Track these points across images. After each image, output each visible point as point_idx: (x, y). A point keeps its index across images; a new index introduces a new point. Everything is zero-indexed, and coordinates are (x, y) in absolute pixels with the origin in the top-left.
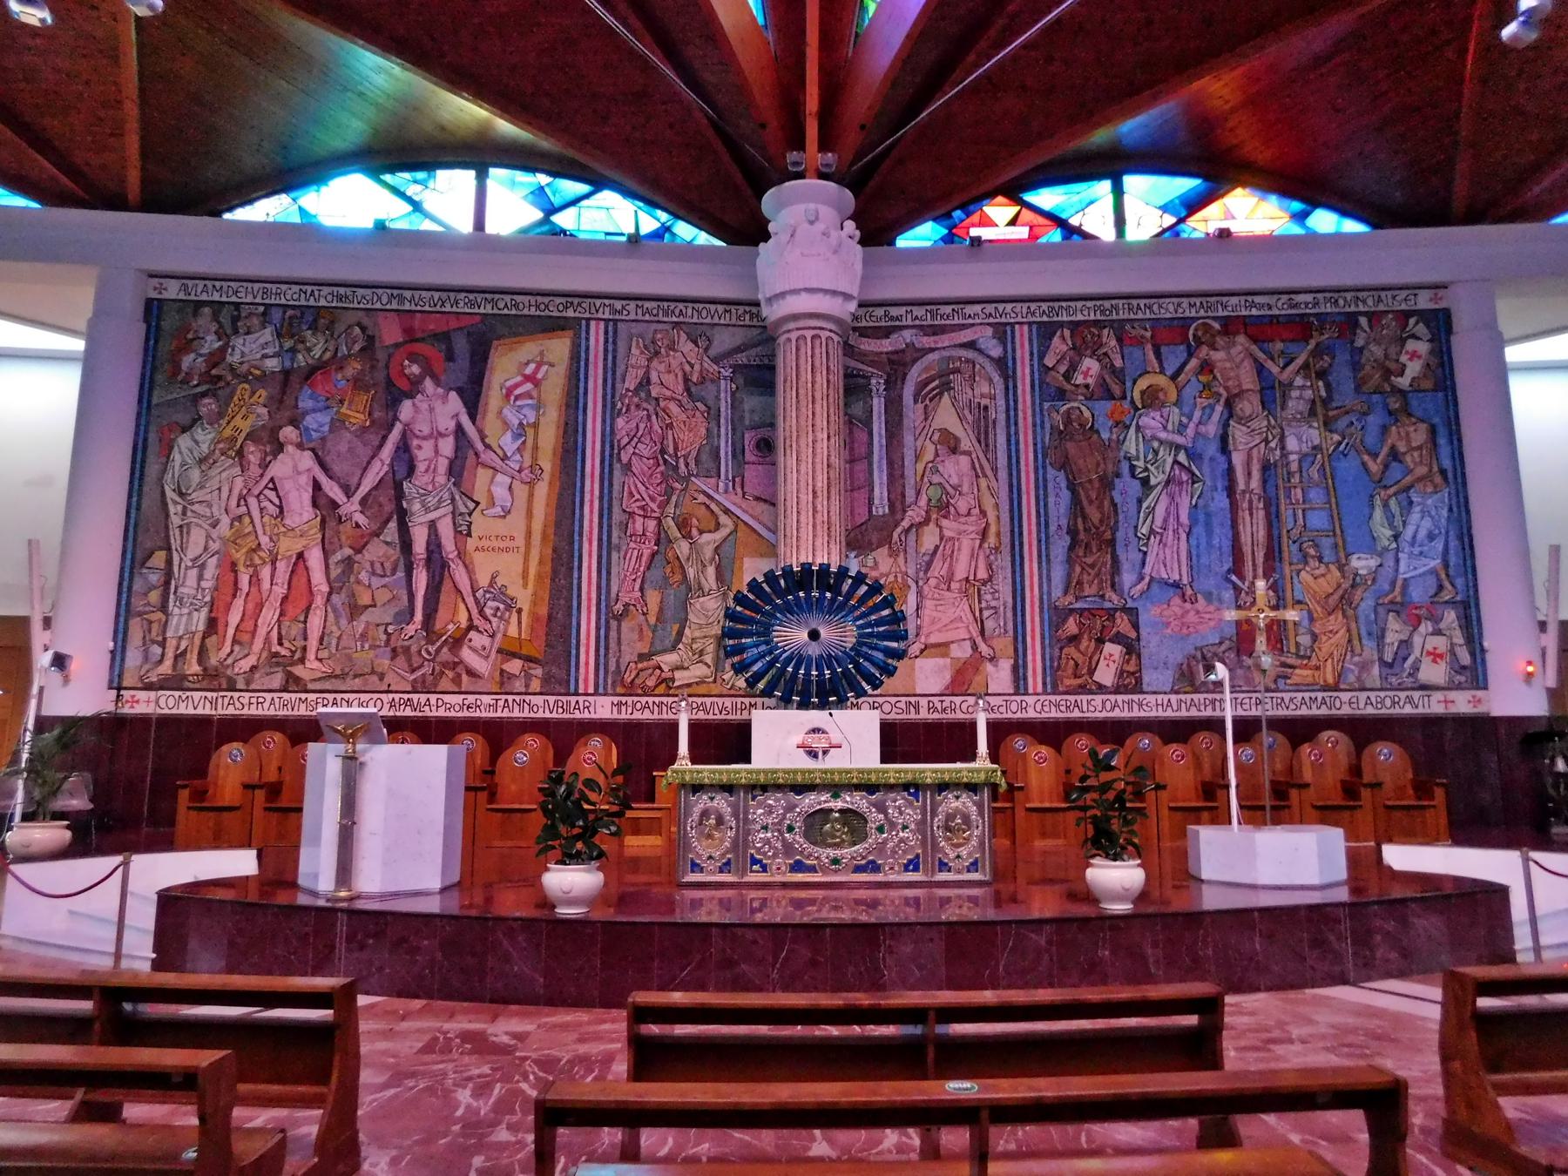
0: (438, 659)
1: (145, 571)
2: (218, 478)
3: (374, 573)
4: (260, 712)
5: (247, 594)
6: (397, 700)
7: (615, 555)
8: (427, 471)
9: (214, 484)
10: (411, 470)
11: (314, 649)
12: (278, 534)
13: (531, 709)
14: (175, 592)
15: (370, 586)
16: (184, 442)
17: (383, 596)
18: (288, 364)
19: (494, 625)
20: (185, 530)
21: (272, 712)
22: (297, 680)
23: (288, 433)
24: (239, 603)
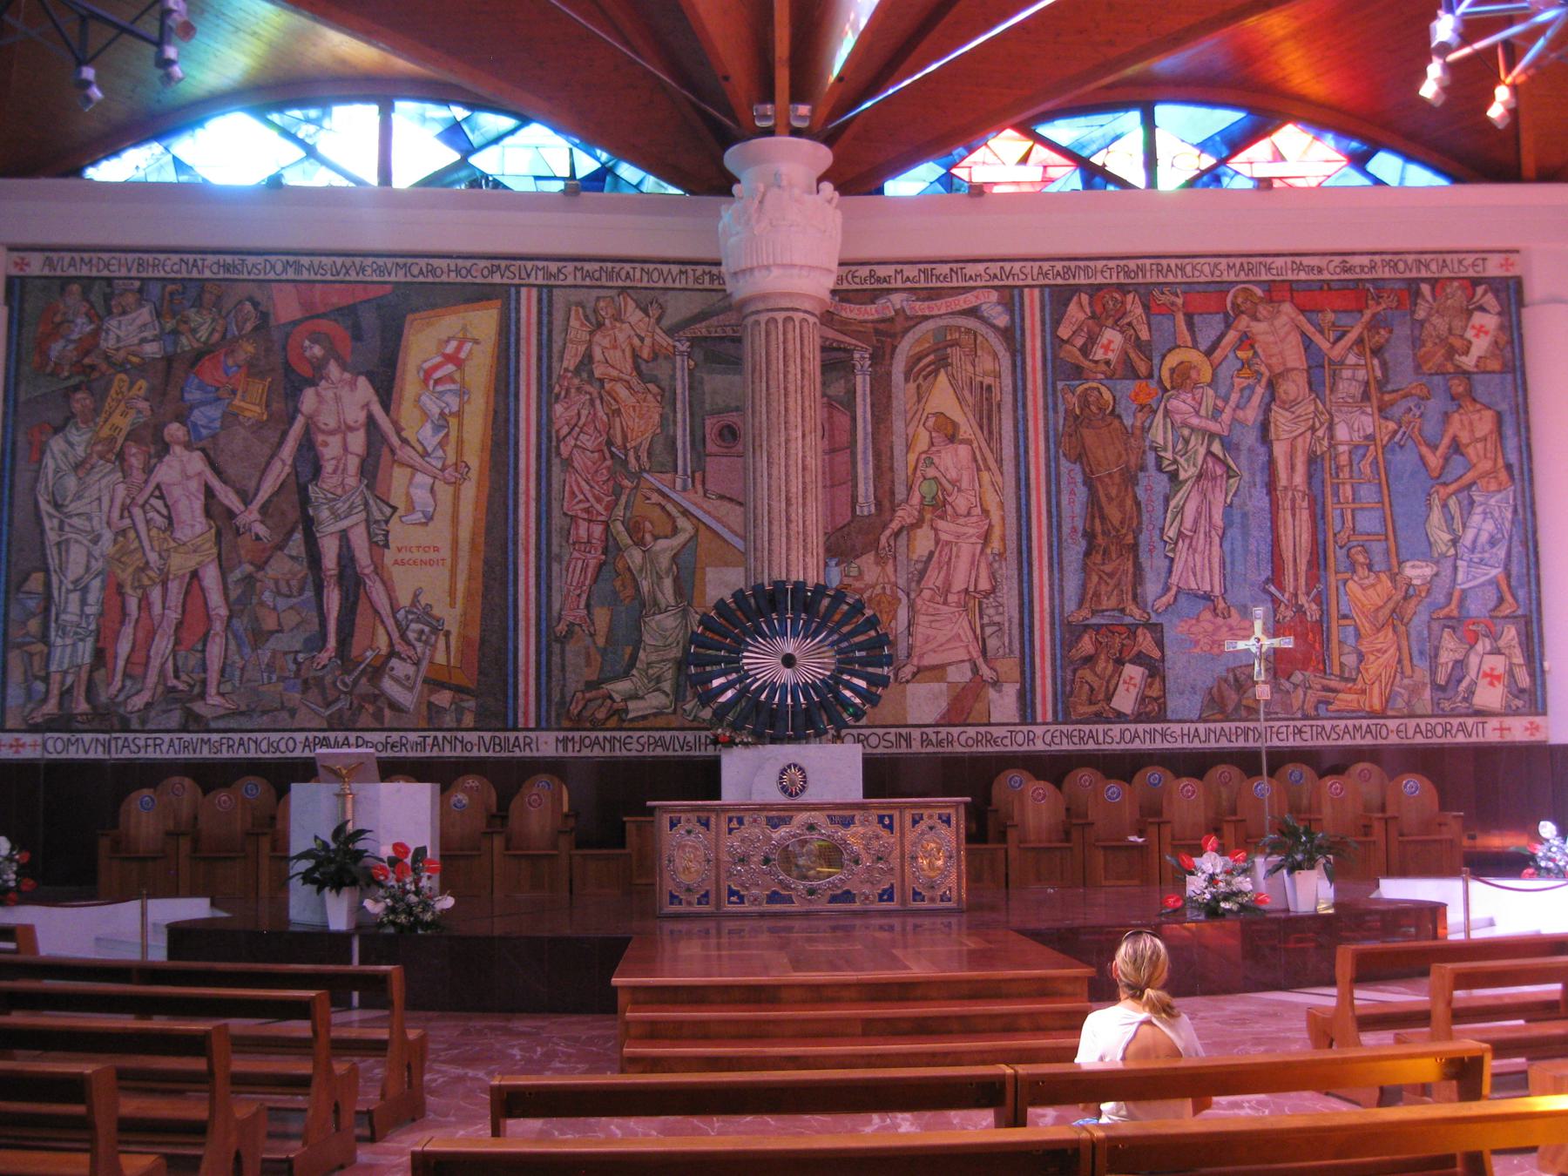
0: (357, 691)
1: (21, 596)
2: (97, 486)
3: (278, 593)
4: (158, 755)
5: (137, 621)
6: (311, 739)
7: (555, 567)
8: (335, 472)
9: (93, 492)
10: (317, 470)
11: (215, 683)
12: (168, 550)
13: (464, 747)
14: (57, 619)
15: (275, 609)
16: (57, 444)
17: (291, 619)
18: (170, 349)
19: (419, 650)
20: (63, 548)
21: (171, 755)
22: (198, 718)
23: (175, 430)
24: (128, 630)
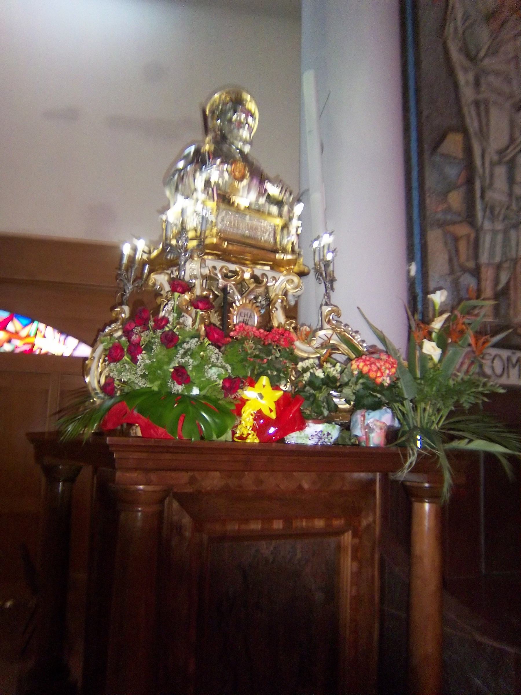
20: (482, 108)
